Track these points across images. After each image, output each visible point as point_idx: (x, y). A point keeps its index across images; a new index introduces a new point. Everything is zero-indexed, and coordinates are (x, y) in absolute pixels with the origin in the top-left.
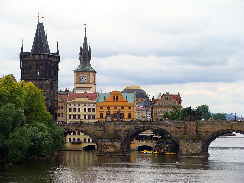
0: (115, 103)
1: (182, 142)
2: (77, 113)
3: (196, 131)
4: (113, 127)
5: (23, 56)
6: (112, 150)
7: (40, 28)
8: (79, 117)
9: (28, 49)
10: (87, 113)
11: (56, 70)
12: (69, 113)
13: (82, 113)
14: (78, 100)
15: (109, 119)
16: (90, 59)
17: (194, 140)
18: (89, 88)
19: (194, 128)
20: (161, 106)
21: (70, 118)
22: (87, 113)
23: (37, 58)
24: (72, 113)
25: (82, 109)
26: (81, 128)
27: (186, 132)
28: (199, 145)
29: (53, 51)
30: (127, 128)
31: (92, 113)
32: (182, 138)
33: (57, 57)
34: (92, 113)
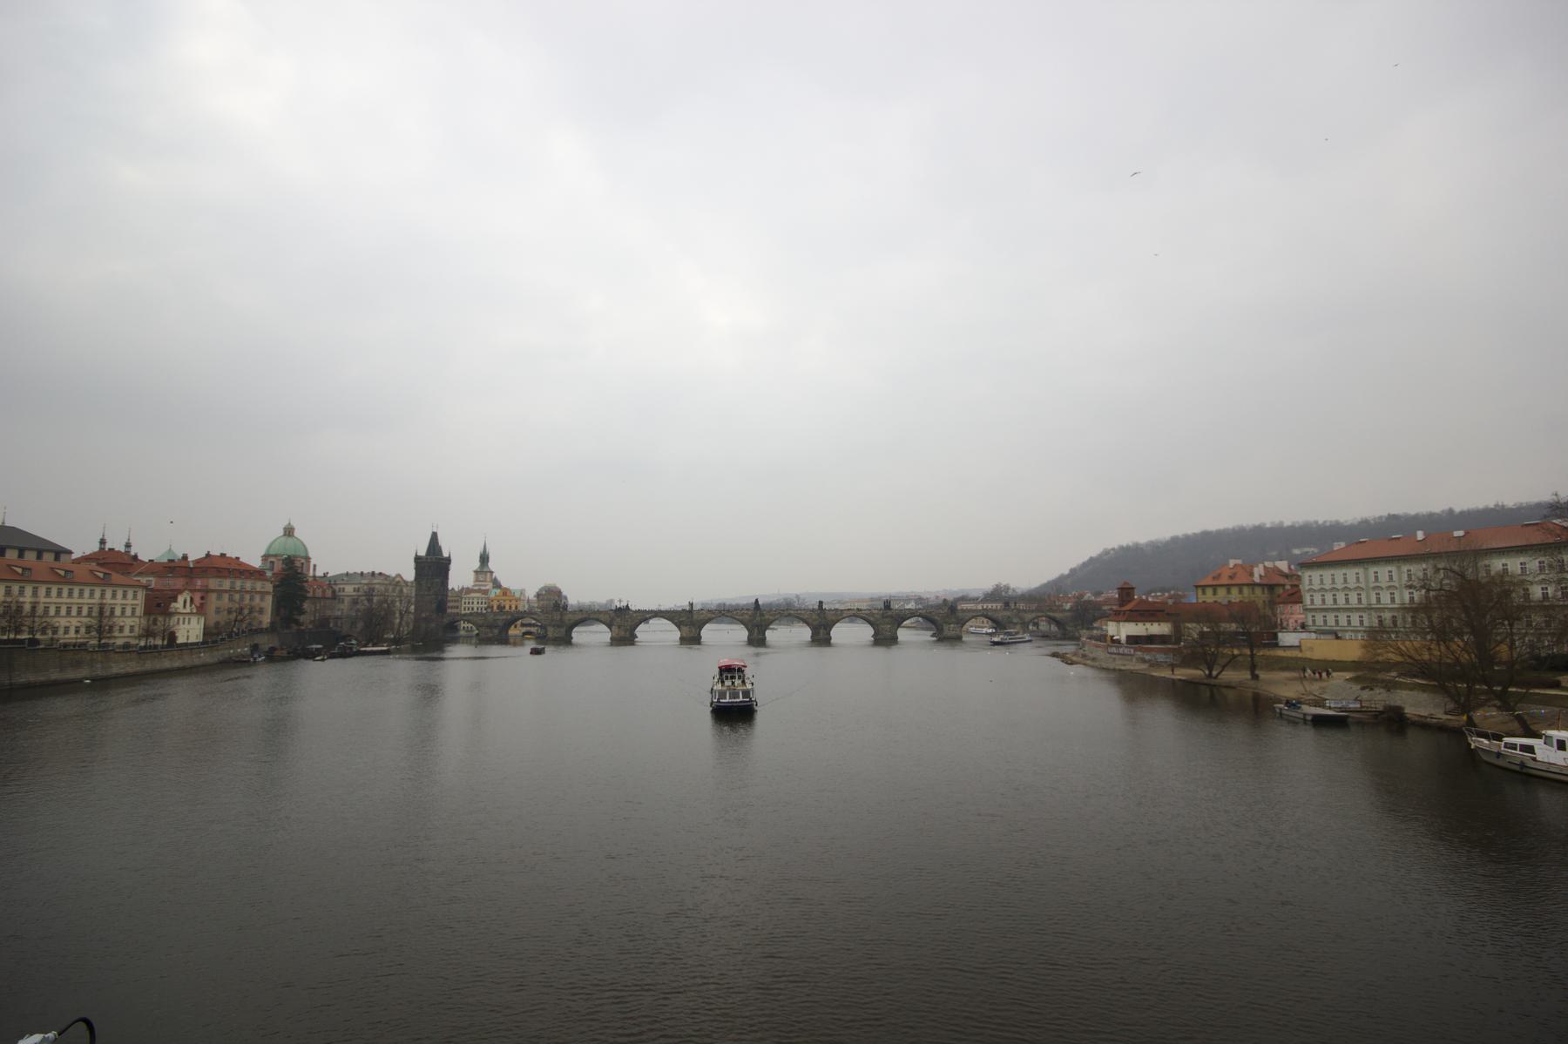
0: (504, 598)
3: (561, 619)
4: (492, 616)
5: (418, 559)
6: (490, 635)
7: (434, 537)
8: (473, 609)
9: (423, 553)
11: (448, 570)
12: (463, 606)
13: (475, 606)
14: (473, 595)
16: (488, 561)
17: (558, 626)
18: (485, 586)
19: (559, 617)
21: (465, 609)
23: (429, 560)
24: (467, 605)
25: (475, 603)
26: (465, 618)
27: (552, 620)
28: (563, 630)
29: (445, 554)
30: (504, 617)
33: (448, 560)
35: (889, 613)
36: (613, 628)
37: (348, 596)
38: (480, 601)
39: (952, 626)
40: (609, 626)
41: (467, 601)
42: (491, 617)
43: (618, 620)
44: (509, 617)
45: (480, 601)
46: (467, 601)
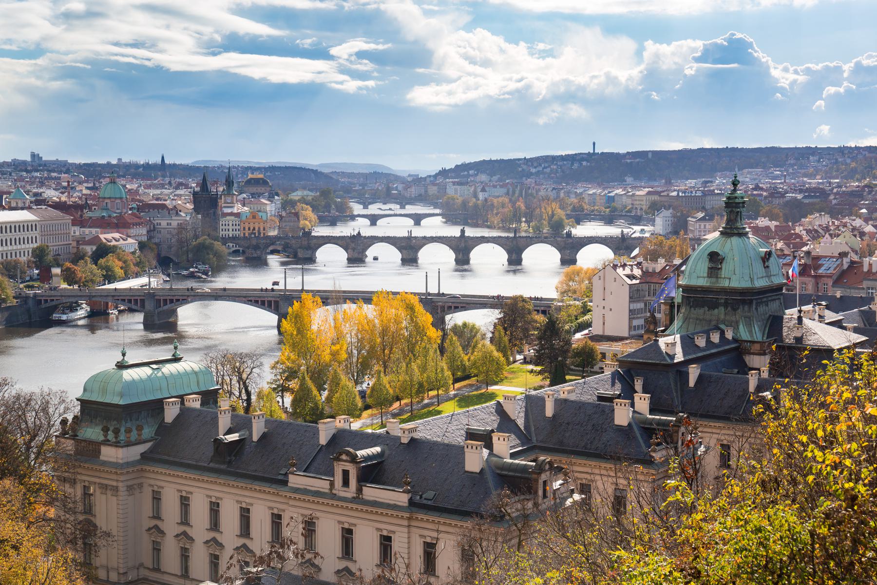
0: (254, 220)
1: (299, 250)
2: (227, 227)
6: (256, 255)
10: (234, 227)
13: (231, 228)
14: (228, 218)
15: (253, 236)
17: (307, 250)
19: (306, 243)
20: (285, 221)
22: (234, 227)
25: (231, 225)
31: (238, 227)
32: (300, 248)
34: (238, 227)
35: (570, 241)
36: (349, 250)
37: (164, 228)
38: (234, 223)
39: (621, 251)
40: (346, 249)
41: (224, 223)
42: (254, 242)
43: (353, 245)
44: (268, 241)
45: (234, 223)
46: (224, 223)
